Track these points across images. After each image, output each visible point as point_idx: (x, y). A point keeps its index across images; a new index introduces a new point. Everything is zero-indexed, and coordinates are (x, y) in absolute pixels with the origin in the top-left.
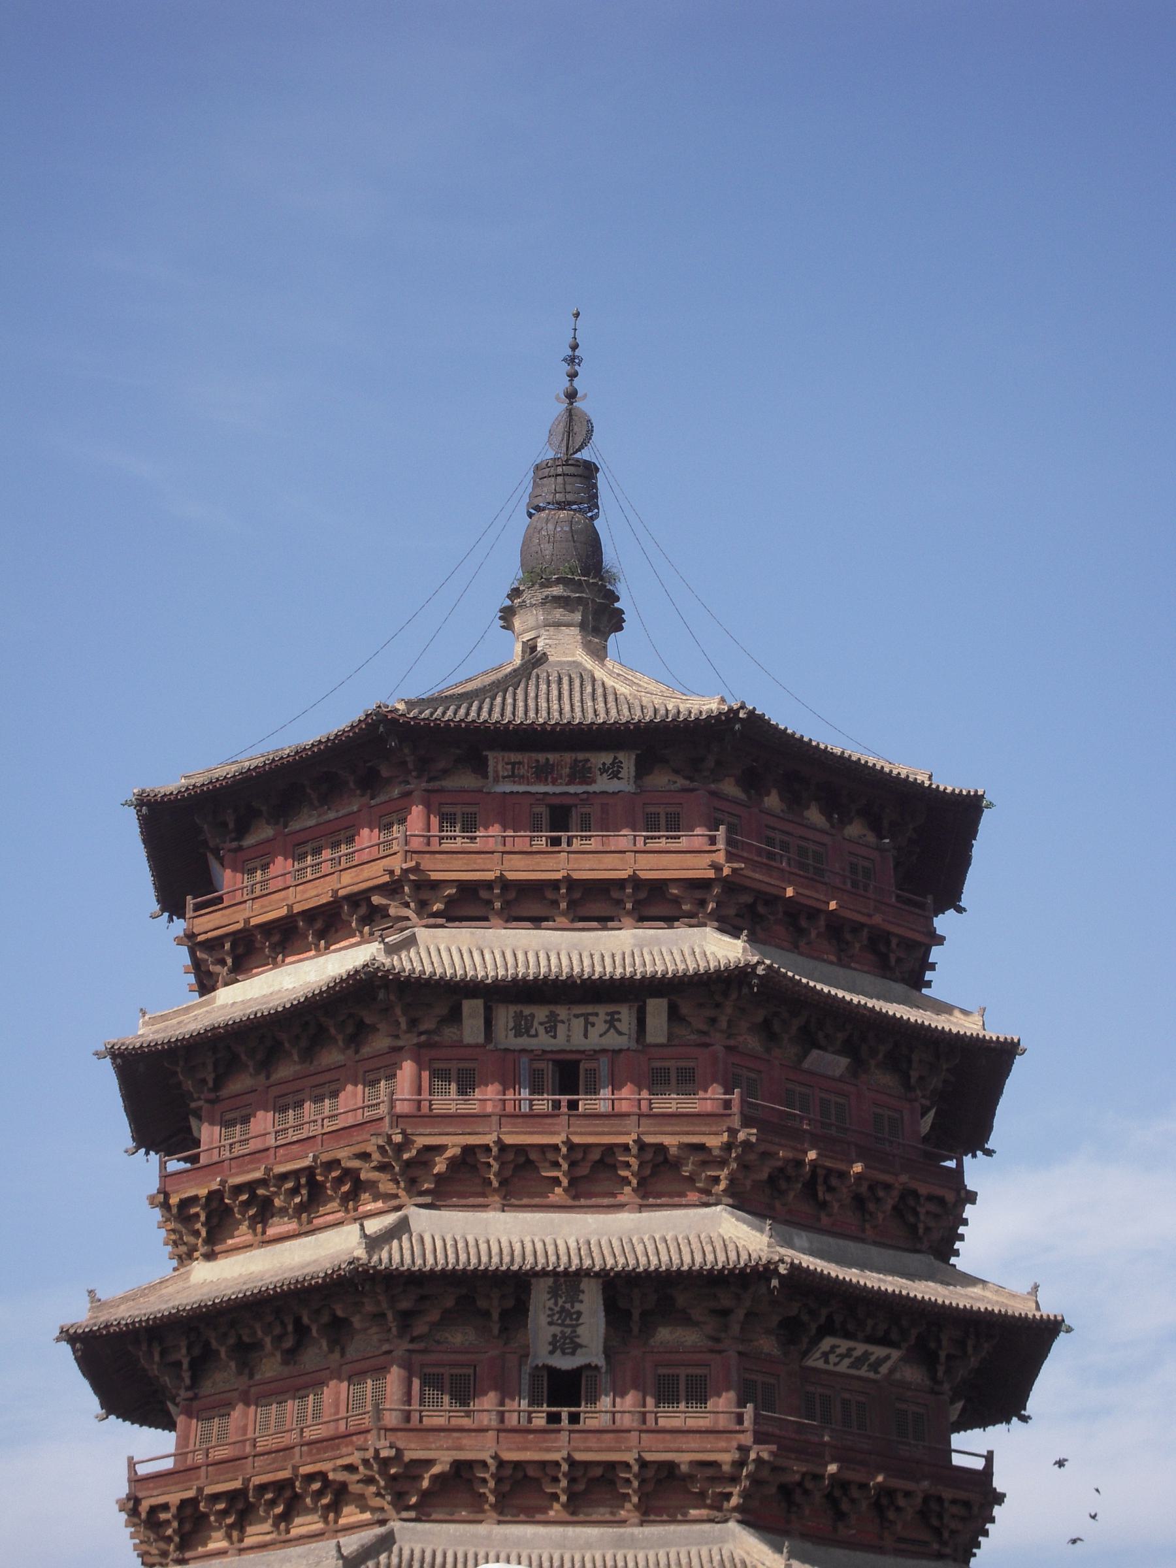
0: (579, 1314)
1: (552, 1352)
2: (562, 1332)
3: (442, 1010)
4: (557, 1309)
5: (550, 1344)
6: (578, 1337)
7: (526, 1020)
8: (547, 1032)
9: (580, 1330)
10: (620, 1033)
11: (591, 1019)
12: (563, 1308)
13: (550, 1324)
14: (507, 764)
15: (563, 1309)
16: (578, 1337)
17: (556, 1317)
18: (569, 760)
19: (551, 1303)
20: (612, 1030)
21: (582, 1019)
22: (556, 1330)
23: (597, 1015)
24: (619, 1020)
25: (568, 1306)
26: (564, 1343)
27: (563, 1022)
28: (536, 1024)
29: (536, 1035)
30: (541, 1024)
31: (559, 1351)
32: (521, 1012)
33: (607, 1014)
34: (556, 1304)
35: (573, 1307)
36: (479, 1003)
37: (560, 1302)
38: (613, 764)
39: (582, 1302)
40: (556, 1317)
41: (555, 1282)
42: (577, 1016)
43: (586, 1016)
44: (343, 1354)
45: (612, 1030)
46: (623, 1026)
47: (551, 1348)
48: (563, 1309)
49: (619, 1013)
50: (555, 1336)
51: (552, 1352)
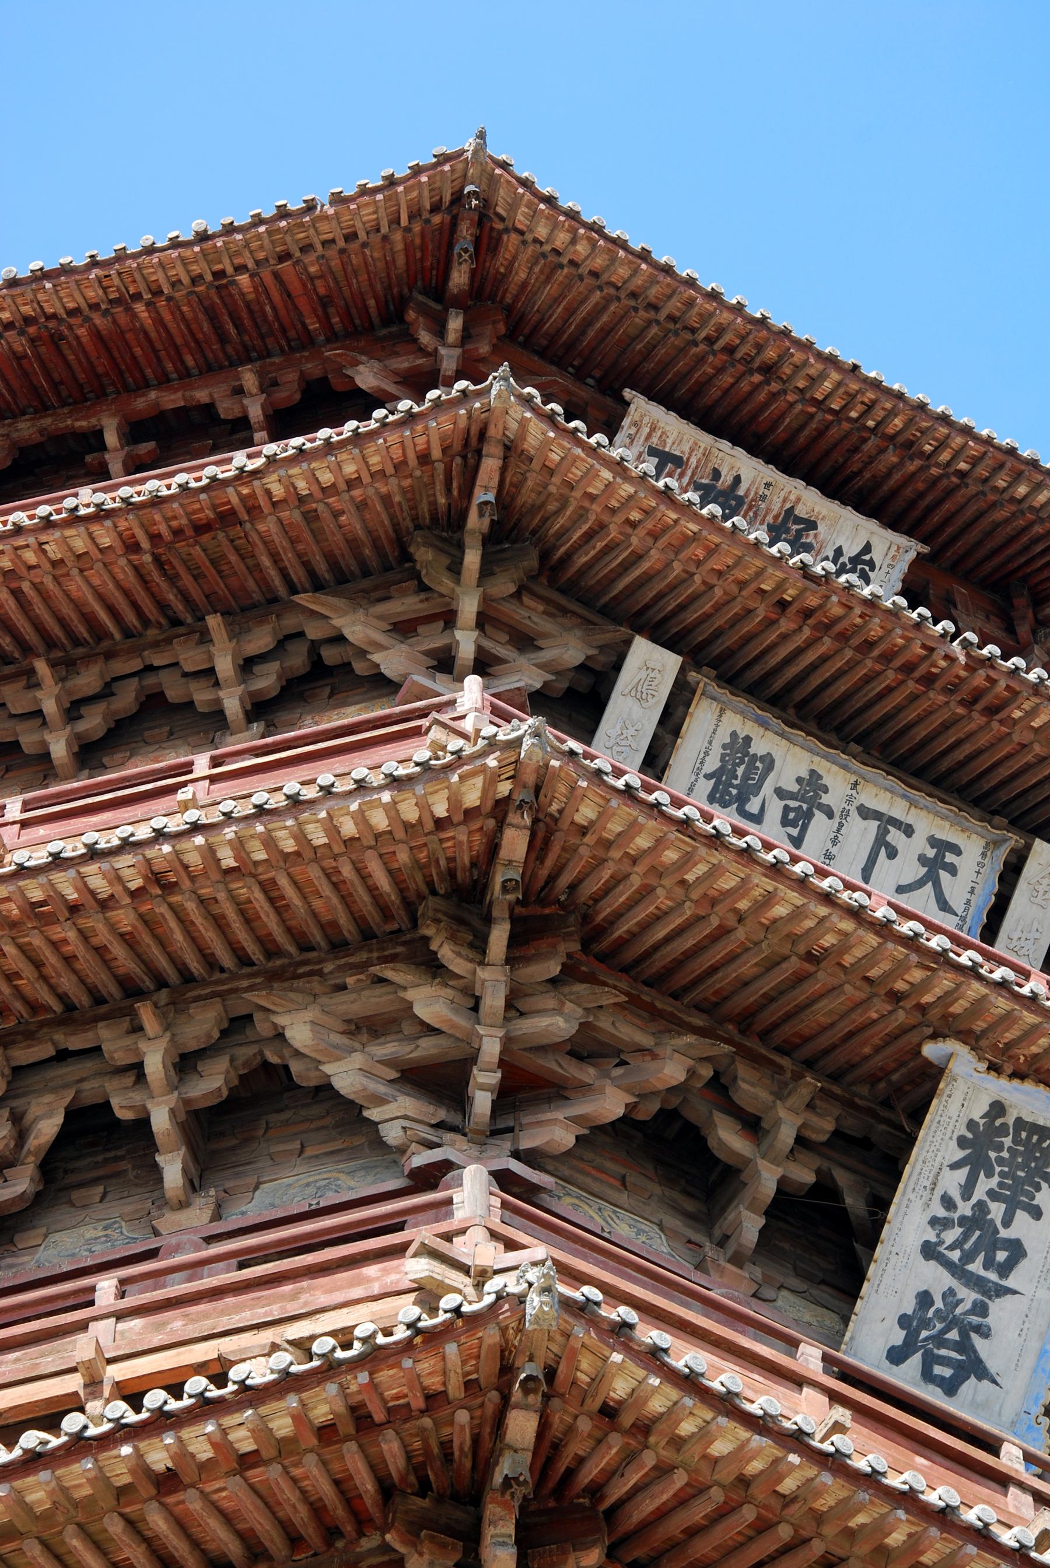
0: (1017, 1250)
1: (896, 1356)
2: (951, 1292)
3: (569, 649)
4: (965, 1209)
5: (904, 1321)
6: (984, 1332)
7: (751, 768)
8: (785, 822)
9: (1000, 1311)
10: (944, 905)
11: (895, 836)
12: (981, 1206)
13: (929, 1251)
14: (653, 452)
15: (978, 1220)
16: (984, 1332)
17: (952, 1235)
18: (776, 508)
19: (953, 1181)
20: (929, 887)
21: (873, 825)
22: (937, 1279)
23: (909, 831)
24: (953, 870)
25: (997, 1210)
26: (939, 1340)
27: (830, 815)
28: (768, 789)
29: (757, 819)
30: (780, 793)
31: (915, 1360)
32: (748, 740)
33: (933, 842)
34: (967, 1191)
35: (1007, 1222)
36: (670, 662)
37: (984, 1185)
38: (855, 560)
39: (1036, 1213)
40: (952, 1235)
41: (998, 1109)
42: (865, 813)
43: (887, 822)
44: (217, 1216)
45: (929, 887)
46: (956, 889)
47: (898, 1337)
48: (978, 1220)
49: (957, 851)
50: (925, 1299)
51: (896, 1356)
